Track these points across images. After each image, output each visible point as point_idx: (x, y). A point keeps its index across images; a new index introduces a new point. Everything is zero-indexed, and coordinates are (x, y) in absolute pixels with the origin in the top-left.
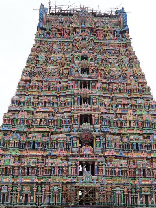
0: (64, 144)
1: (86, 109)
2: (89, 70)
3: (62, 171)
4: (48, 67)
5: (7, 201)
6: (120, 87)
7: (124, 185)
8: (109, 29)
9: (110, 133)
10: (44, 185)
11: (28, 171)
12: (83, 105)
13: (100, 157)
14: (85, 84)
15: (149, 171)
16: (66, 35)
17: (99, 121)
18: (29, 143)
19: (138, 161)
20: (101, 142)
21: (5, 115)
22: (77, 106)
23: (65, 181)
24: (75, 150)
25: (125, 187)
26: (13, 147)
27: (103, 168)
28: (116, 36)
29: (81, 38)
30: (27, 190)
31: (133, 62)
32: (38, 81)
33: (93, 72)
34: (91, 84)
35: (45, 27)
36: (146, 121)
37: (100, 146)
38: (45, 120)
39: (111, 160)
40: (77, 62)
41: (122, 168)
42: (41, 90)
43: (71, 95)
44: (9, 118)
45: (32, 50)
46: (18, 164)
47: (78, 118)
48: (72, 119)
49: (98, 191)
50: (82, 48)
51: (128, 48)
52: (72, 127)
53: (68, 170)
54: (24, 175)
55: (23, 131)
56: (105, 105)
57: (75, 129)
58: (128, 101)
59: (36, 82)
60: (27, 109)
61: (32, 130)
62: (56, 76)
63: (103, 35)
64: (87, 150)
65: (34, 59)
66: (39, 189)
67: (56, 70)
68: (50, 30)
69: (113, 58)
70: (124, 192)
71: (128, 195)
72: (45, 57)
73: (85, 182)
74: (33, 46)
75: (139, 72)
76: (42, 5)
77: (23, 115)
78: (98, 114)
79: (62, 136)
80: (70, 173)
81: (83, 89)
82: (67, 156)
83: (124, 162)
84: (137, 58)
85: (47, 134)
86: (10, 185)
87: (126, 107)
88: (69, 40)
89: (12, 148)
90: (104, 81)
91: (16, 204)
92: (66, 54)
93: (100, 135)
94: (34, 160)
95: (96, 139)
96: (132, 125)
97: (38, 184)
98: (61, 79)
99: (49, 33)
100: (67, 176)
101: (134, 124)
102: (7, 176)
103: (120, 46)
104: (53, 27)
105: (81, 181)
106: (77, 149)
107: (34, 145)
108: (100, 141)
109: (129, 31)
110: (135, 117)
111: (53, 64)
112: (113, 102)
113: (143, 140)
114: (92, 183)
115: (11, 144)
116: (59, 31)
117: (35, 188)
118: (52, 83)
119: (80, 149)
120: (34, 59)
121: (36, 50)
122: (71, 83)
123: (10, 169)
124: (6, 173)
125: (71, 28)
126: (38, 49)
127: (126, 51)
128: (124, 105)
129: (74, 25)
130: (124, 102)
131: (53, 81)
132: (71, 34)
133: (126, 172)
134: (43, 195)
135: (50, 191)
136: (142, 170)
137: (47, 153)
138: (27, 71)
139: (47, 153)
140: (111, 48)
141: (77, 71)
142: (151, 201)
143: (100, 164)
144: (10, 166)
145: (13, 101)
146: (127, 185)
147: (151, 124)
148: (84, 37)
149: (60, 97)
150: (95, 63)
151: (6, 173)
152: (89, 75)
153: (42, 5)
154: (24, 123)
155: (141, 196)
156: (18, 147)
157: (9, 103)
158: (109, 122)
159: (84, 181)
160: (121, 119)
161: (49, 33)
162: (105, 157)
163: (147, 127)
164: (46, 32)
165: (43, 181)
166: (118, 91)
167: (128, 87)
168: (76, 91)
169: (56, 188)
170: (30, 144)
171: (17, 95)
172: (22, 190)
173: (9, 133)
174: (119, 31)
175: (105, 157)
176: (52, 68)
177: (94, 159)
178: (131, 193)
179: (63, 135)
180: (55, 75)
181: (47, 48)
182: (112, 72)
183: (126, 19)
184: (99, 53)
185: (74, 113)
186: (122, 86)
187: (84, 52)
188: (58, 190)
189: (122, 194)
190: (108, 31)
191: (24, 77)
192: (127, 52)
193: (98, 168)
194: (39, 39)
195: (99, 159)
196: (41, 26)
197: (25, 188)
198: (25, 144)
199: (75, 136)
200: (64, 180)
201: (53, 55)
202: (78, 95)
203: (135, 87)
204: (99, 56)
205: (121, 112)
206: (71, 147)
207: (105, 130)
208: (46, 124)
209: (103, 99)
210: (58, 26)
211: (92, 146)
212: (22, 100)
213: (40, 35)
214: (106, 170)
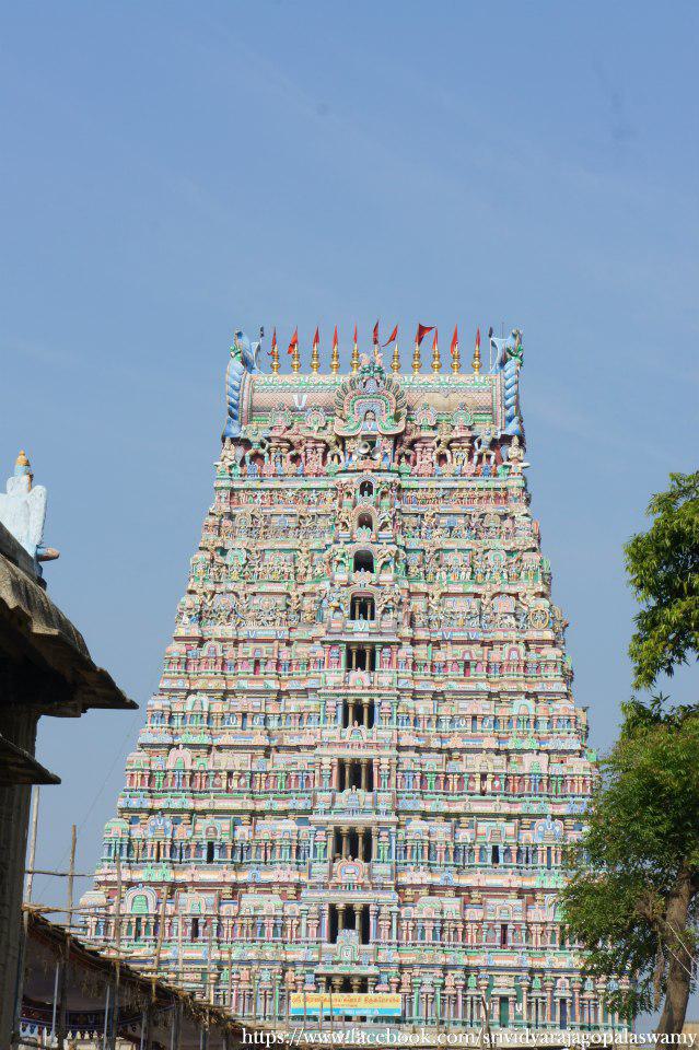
0: (291, 849)
1: (357, 743)
2: (377, 604)
3: (283, 928)
6: (467, 657)
7: (445, 968)
8: (454, 436)
9: (425, 815)
12: (350, 728)
13: (384, 888)
14: (360, 657)
16: (315, 464)
19: (490, 901)
24: (320, 869)
25: (450, 972)
26: (154, 858)
27: (391, 921)
28: (475, 459)
29: (356, 480)
33: (385, 611)
34: (378, 654)
36: (530, 775)
41: (443, 921)
42: (233, 672)
44: (143, 770)
46: (170, 909)
47: (331, 771)
48: (317, 772)
55: (182, 811)
57: (321, 806)
62: (277, 622)
63: (434, 458)
64: (351, 870)
65: (212, 560)
67: (280, 600)
68: (263, 445)
71: (456, 995)
73: (341, 962)
79: (288, 828)
82: (299, 886)
83: (452, 905)
89: (151, 861)
93: (392, 823)
94: (211, 897)
95: (379, 836)
97: (220, 964)
102: (142, 943)
103: (488, 497)
104: (272, 434)
108: (390, 842)
111: (272, 578)
112: (444, 710)
114: (358, 963)
115: (149, 850)
118: (263, 646)
119: (331, 868)
120: (212, 560)
123: (147, 923)
125: (331, 439)
126: (226, 522)
127: (504, 517)
132: (329, 459)
133: (456, 929)
134: (234, 994)
136: (498, 926)
141: (337, 609)
142: (515, 1011)
143: (384, 910)
144: (147, 915)
146: (455, 967)
147: (545, 782)
148: (368, 475)
150: (396, 580)
151: (138, 933)
152: (373, 624)
154: (184, 784)
156: (168, 858)
159: (336, 959)
160: (461, 768)
162: (399, 888)
163: (532, 791)
164: (251, 451)
169: (266, 976)
173: (144, 815)
174: (489, 438)
175: (399, 888)
178: (466, 987)
179: (289, 825)
180: (274, 620)
181: (253, 516)
182: (449, 601)
186: (476, 649)
187: (364, 539)
190: (451, 441)
192: (508, 523)
198: (188, 847)
202: (338, 695)
203: (514, 655)
207: (410, 807)
210: (289, 428)
213: (230, 467)
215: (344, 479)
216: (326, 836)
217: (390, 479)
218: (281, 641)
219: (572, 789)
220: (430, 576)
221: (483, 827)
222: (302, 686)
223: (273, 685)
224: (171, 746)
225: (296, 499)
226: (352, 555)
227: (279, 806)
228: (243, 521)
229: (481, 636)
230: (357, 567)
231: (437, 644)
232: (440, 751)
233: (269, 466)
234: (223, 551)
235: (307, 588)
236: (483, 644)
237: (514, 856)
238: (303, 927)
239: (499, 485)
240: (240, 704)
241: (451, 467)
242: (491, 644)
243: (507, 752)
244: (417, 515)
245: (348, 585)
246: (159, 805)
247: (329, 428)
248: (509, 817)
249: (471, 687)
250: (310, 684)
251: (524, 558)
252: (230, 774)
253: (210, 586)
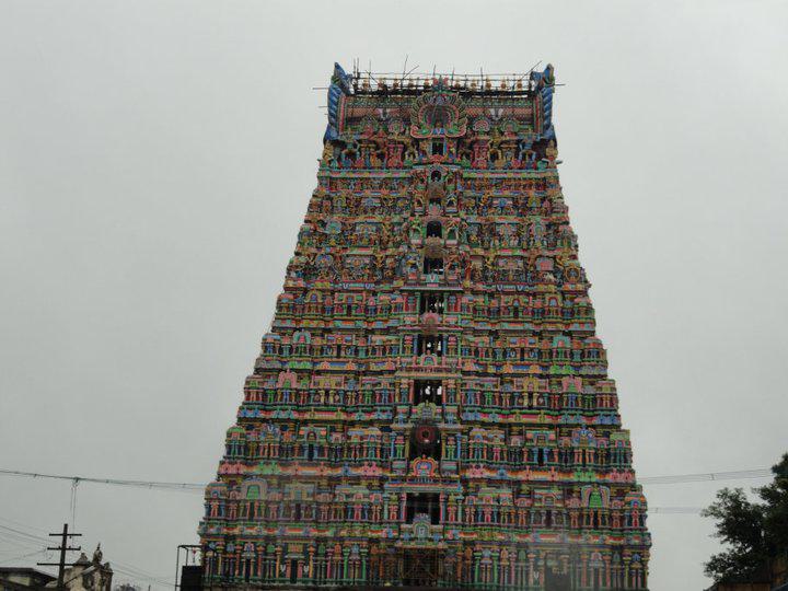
3: (370, 511)
4: (348, 252)
5: (256, 574)
6: (516, 304)
7: (501, 544)
8: (504, 138)
9: (483, 424)
10: (330, 543)
11: (298, 512)
12: (423, 356)
13: (452, 481)
14: (428, 301)
15: (560, 513)
17: (458, 396)
18: (301, 448)
19: (537, 491)
20: (459, 448)
21: (247, 383)
22: (409, 360)
23: (375, 535)
26: (266, 456)
29: (429, 170)
30: (295, 551)
31: (557, 231)
32: (323, 291)
35: (344, 139)
37: (456, 456)
38: (337, 392)
39: (477, 489)
40: (415, 241)
43: (395, 330)
45: (311, 206)
46: (275, 495)
48: (397, 390)
49: (443, 557)
50: (432, 201)
51: (549, 192)
52: (395, 412)
53: (382, 510)
54: (289, 521)
56: (477, 352)
58: (532, 340)
59: (319, 294)
60: (296, 366)
61: (307, 416)
62: (366, 277)
64: (423, 467)
65: (315, 230)
66: (321, 550)
68: (355, 146)
69: (506, 223)
70: (500, 559)
72: (340, 226)
74: (314, 196)
75: (568, 262)
76: (337, 66)
77: (288, 381)
78: (456, 379)
80: (386, 516)
81: (426, 315)
82: (382, 479)
84: (567, 223)
85: (340, 426)
86: (261, 542)
87: (526, 357)
88: (402, 174)
90: (481, 287)
91: (274, 581)
92: (392, 214)
93: (456, 430)
94: (310, 488)
95: (447, 440)
96: (535, 404)
97: (318, 540)
98: (377, 283)
99: (351, 155)
100: (381, 523)
101: (541, 400)
103: (531, 185)
104: (362, 137)
105: (405, 536)
106: (403, 465)
107: (311, 453)
109: (555, 141)
110: (543, 382)
111: (361, 244)
112: (497, 345)
113: (555, 441)
114: (431, 540)
116: (377, 148)
117: (312, 549)
119: (408, 464)
120: (315, 230)
121: (320, 205)
122: (400, 299)
124: (252, 514)
127: (543, 200)
128: (522, 350)
129: (414, 132)
130: (523, 345)
131: (354, 290)
135: (342, 555)
137: (340, 472)
138: (297, 267)
139: (340, 472)
140: (507, 193)
141: (414, 266)
143: (452, 498)
145: (266, 346)
146: (508, 543)
148: (437, 166)
149: (373, 331)
150: (459, 244)
153: (337, 66)
155: (536, 568)
156: (277, 456)
157: (258, 351)
158: (482, 395)
159: (413, 536)
161: (351, 155)
162: (465, 482)
163: (570, 406)
165: (329, 533)
166: (512, 314)
167: (538, 303)
168: (409, 320)
169: (355, 550)
170: (304, 451)
171: (274, 329)
172: (285, 552)
174: (530, 141)
175: (465, 482)
176: (358, 256)
177: (438, 488)
178: (517, 560)
179: (375, 431)
182: (501, 262)
183: (550, 107)
184: (473, 208)
185: (400, 378)
186: (523, 299)
187: (434, 212)
188: (360, 553)
189: (496, 563)
190: (502, 143)
191: (291, 284)
192: (546, 204)
193: (447, 506)
194: (327, 174)
195: (451, 488)
196: (334, 134)
197: (291, 548)
199: (401, 433)
200: (372, 531)
201: (361, 218)
202: (414, 331)
203: (553, 302)
204: (473, 219)
205: (512, 370)
206: (391, 458)
207: (471, 417)
208: (339, 401)
209: (471, 338)
210: (375, 133)
211: (438, 457)
212: (286, 341)
213: (330, 162)
214: (463, 510)
215: (420, 169)
216: (404, 440)
217: (455, 170)
218: (369, 291)
219: (601, 405)
220: (486, 245)
221: (530, 434)
222: (385, 326)
223: (362, 325)
224: (281, 370)
225: (381, 187)
226: (425, 225)
227: (365, 417)
229: (527, 289)
230: (429, 234)
231: (492, 295)
232: (495, 375)
234: (324, 225)
235: (388, 253)
236: (528, 294)
237: (556, 457)
238: (386, 512)
239: (539, 176)
240: (336, 338)
241: (500, 162)
242: (534, 295)
243: (548, 376)
244: (475, 198)
245: (422, 247)
246: (273, 415)
247: (407, 132)
248: (550, 427)
249: (519, 327)
250: (390, 324)
251: (560, 228)
252: (327, 392)
253: (314, 250)
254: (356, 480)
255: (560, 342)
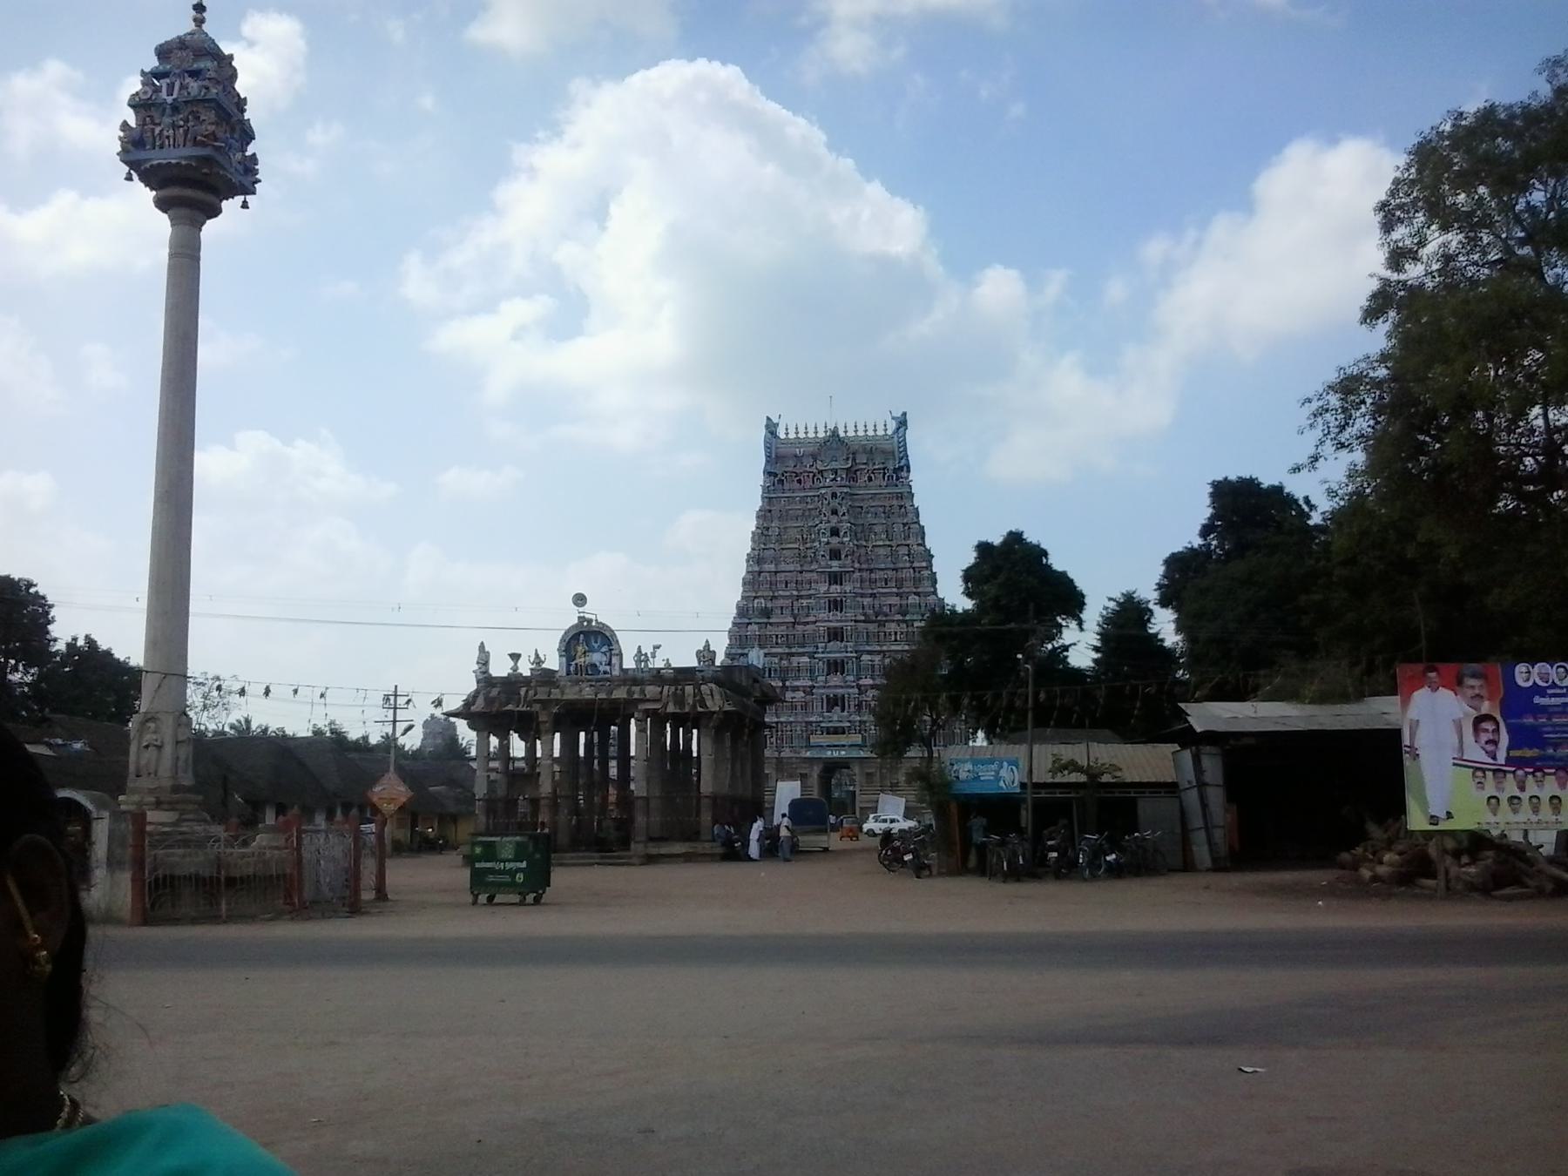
14: (835, 578)
16: (809, 484)
29: (829, 491)
64: (835, 680)
161: (781, 481)
162: (859, 687)
175: (859, 687)
179: (806, 659)
228: (776, 514)
233: (787, 486)
254: (802, 654)
255: (913, 599)
